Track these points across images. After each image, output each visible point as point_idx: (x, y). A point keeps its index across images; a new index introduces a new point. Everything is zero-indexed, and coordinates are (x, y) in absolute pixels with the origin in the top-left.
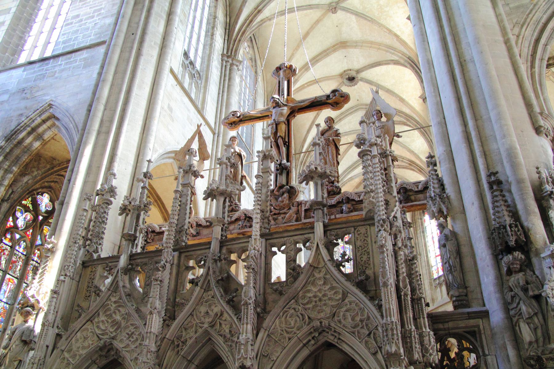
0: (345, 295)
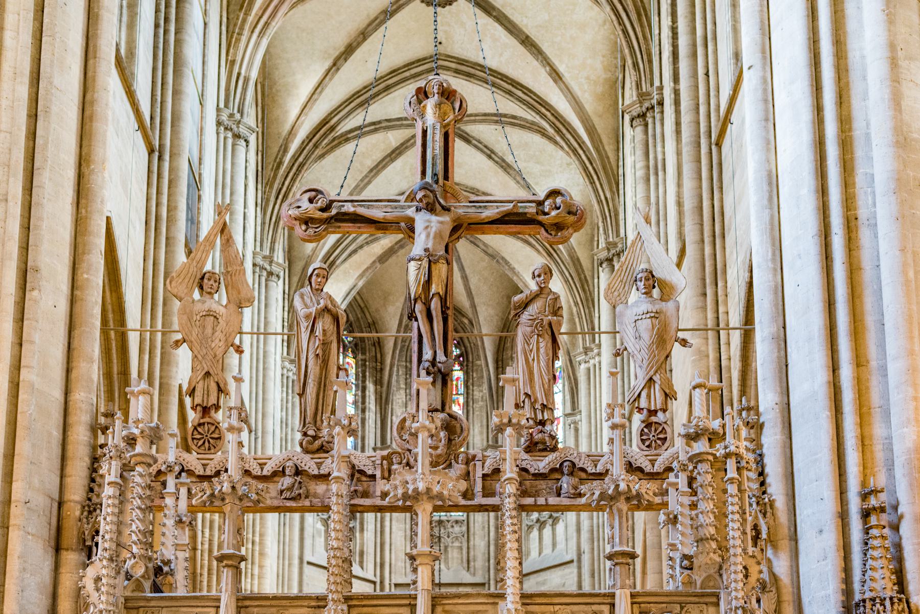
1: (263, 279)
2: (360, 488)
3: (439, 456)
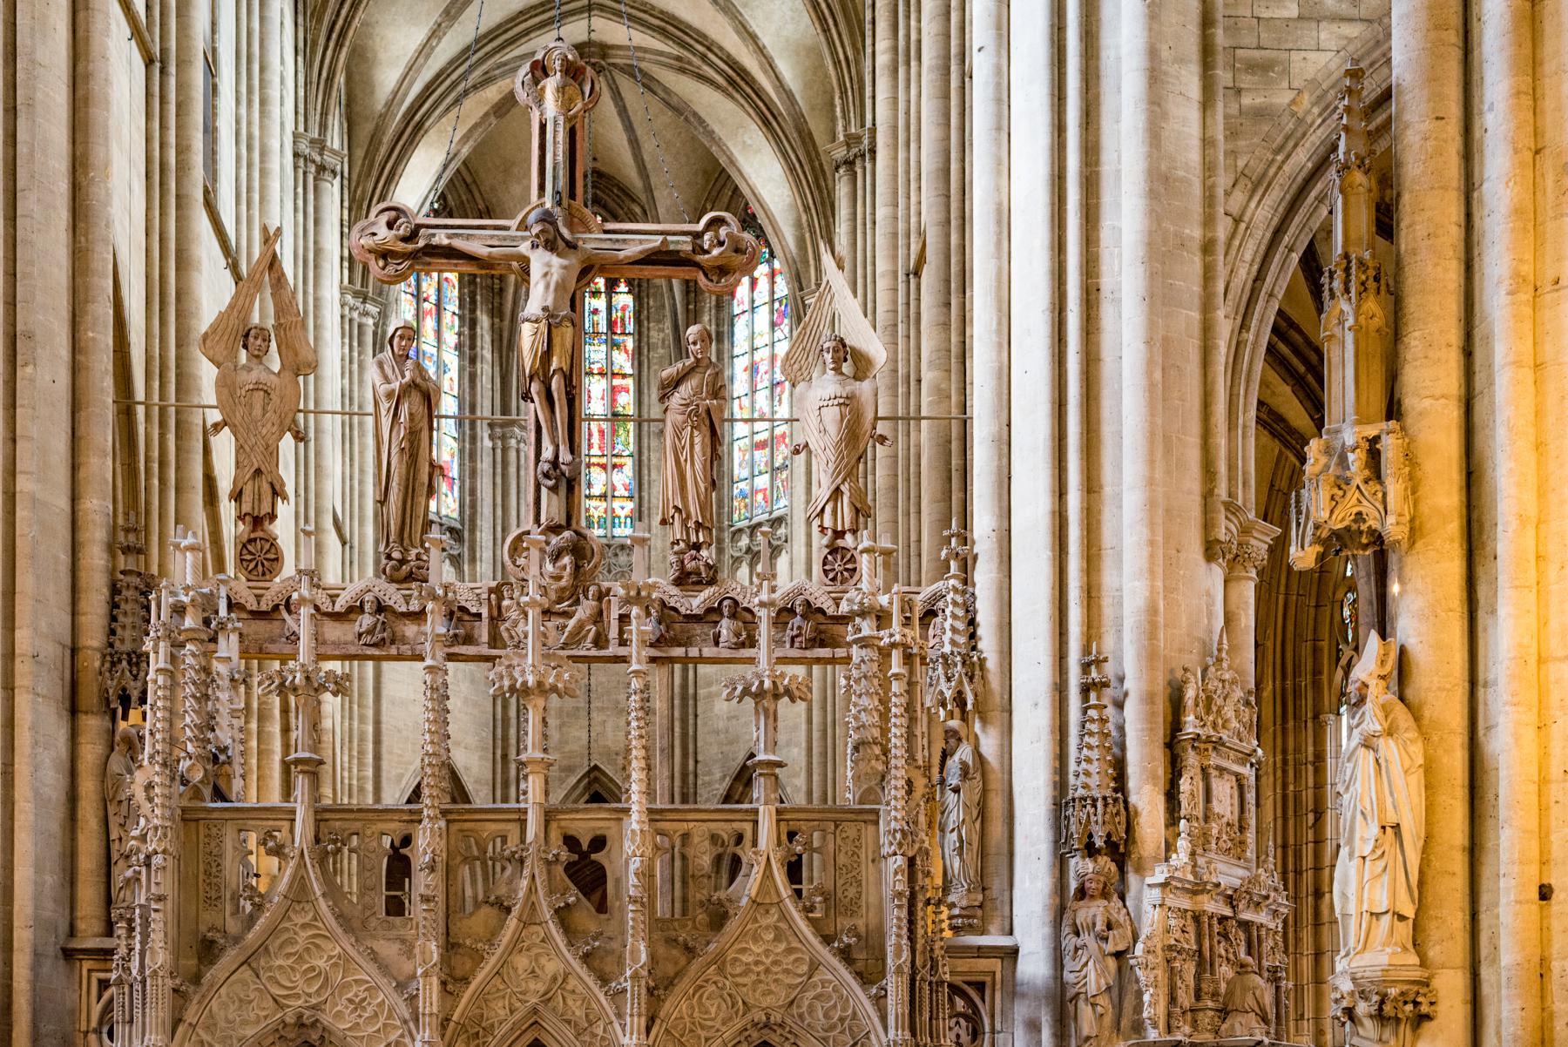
0: (814, 966)
1: (311, 178)
2: (461, 631)
3: (563, 589)
